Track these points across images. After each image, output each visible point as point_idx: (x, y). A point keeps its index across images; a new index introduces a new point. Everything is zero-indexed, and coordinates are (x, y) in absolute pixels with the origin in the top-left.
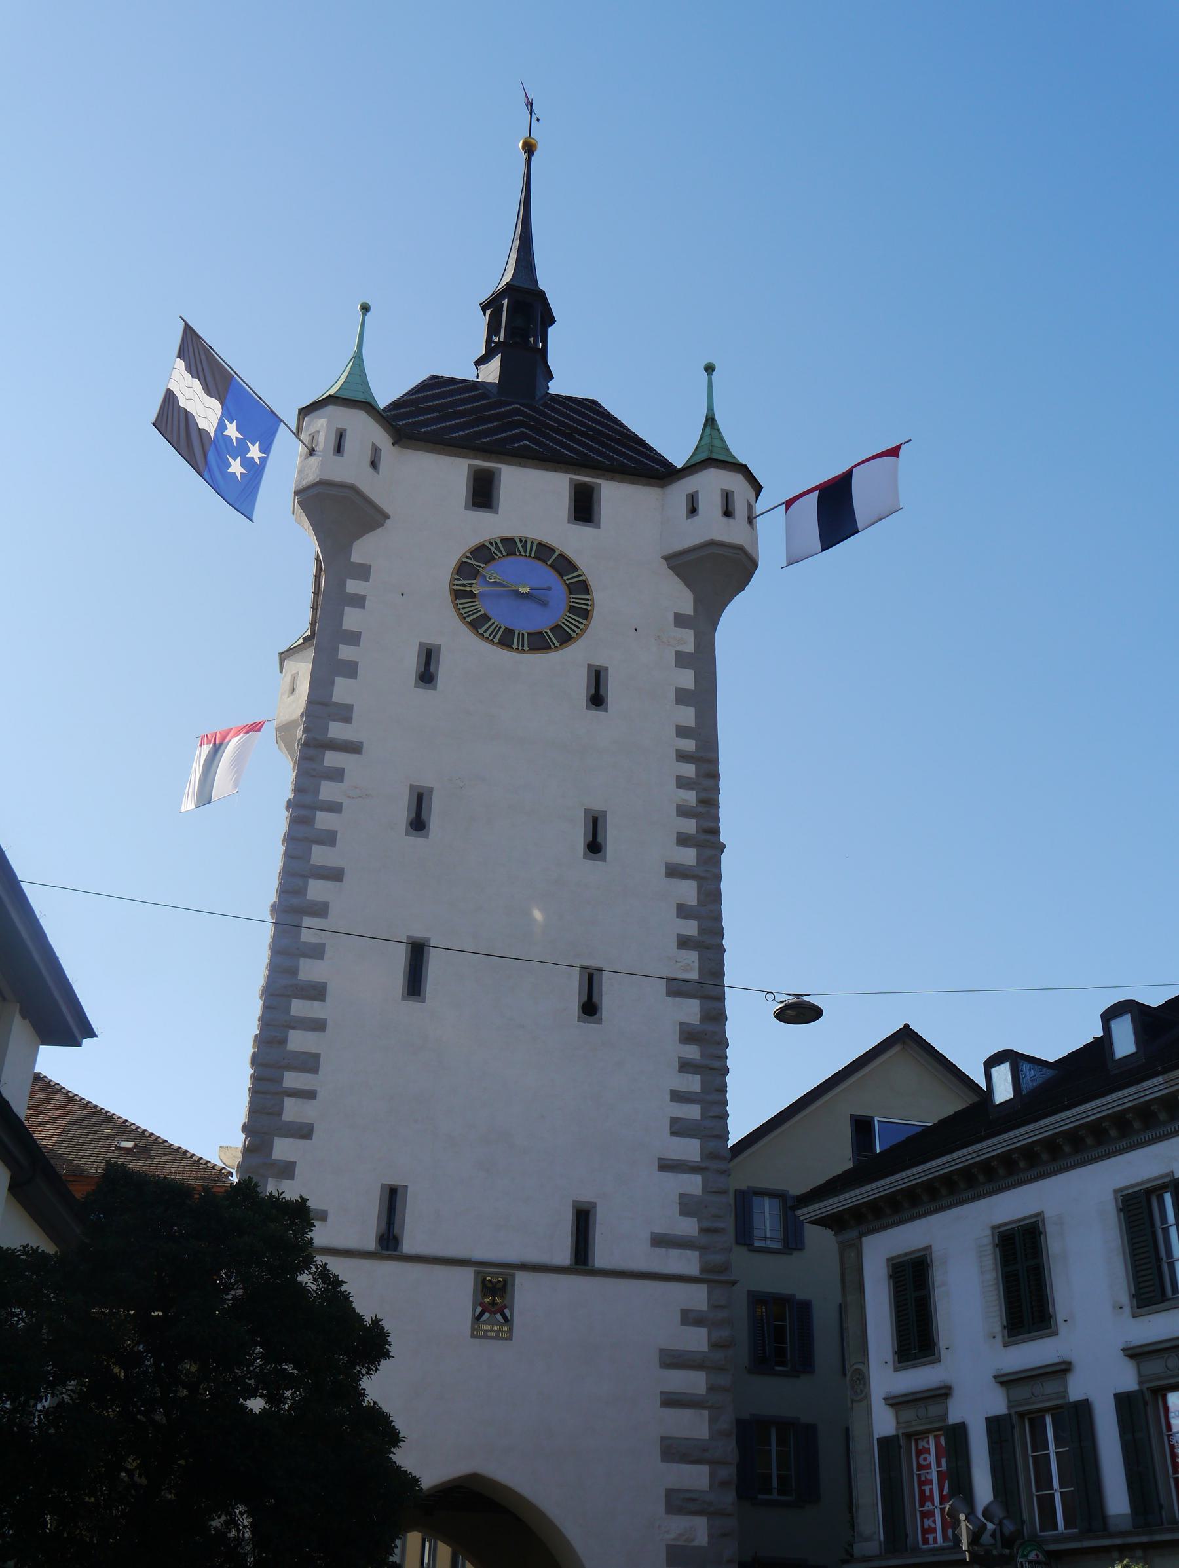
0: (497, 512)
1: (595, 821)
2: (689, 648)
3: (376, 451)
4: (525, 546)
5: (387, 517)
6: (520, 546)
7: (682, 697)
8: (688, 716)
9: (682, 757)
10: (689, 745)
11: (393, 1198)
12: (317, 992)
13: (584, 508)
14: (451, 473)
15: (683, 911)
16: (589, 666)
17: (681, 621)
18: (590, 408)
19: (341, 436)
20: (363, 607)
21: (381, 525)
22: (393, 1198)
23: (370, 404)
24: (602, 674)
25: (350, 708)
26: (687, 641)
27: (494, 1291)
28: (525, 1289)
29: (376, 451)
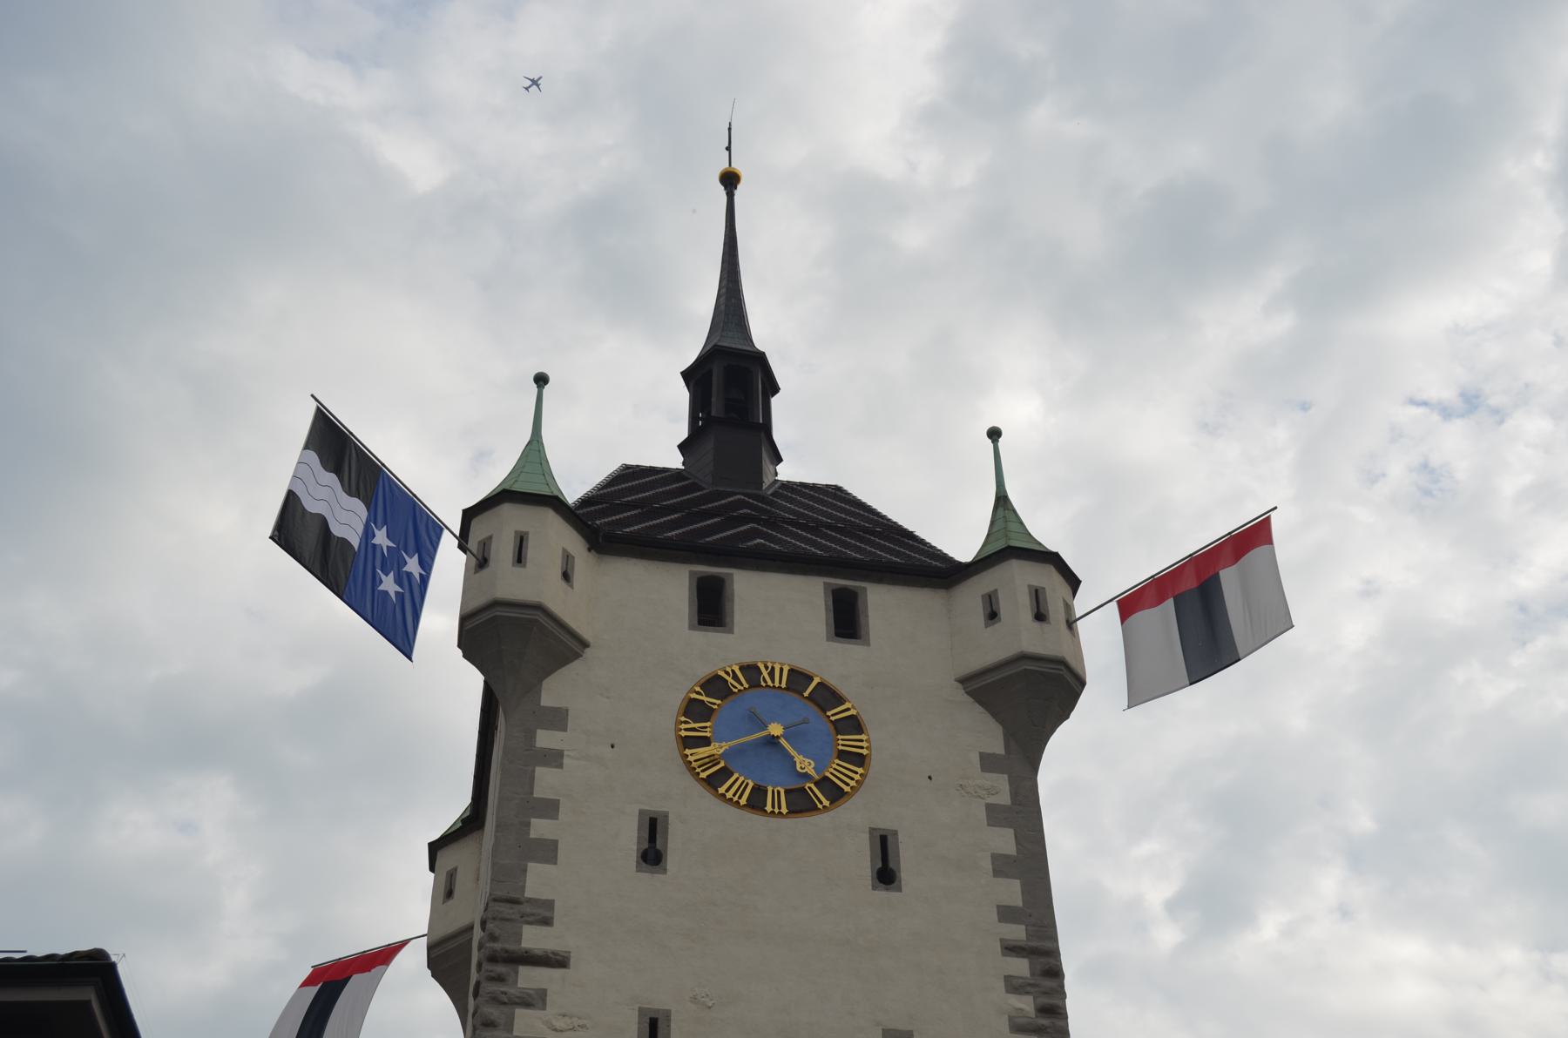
0: (731, 631)
2: (1004, 798)
3: (568, 558)
4: (772, 674)
5: (585, 645)
6: (765, 674)
7: (1002, 865)
8: (1011, 892)
9: (1011, 949)
10: (1017, 933)
13: (847, 621)
16: (872, 830)
17: (989, 763)
18: (835, 497)
19: (521, 541)
20: (560, 766)
21: (577, 656)
23: (556, 498)
24: (890, 839)
25: (549, 905)
26: (1000, 789)
29: (568, 558)
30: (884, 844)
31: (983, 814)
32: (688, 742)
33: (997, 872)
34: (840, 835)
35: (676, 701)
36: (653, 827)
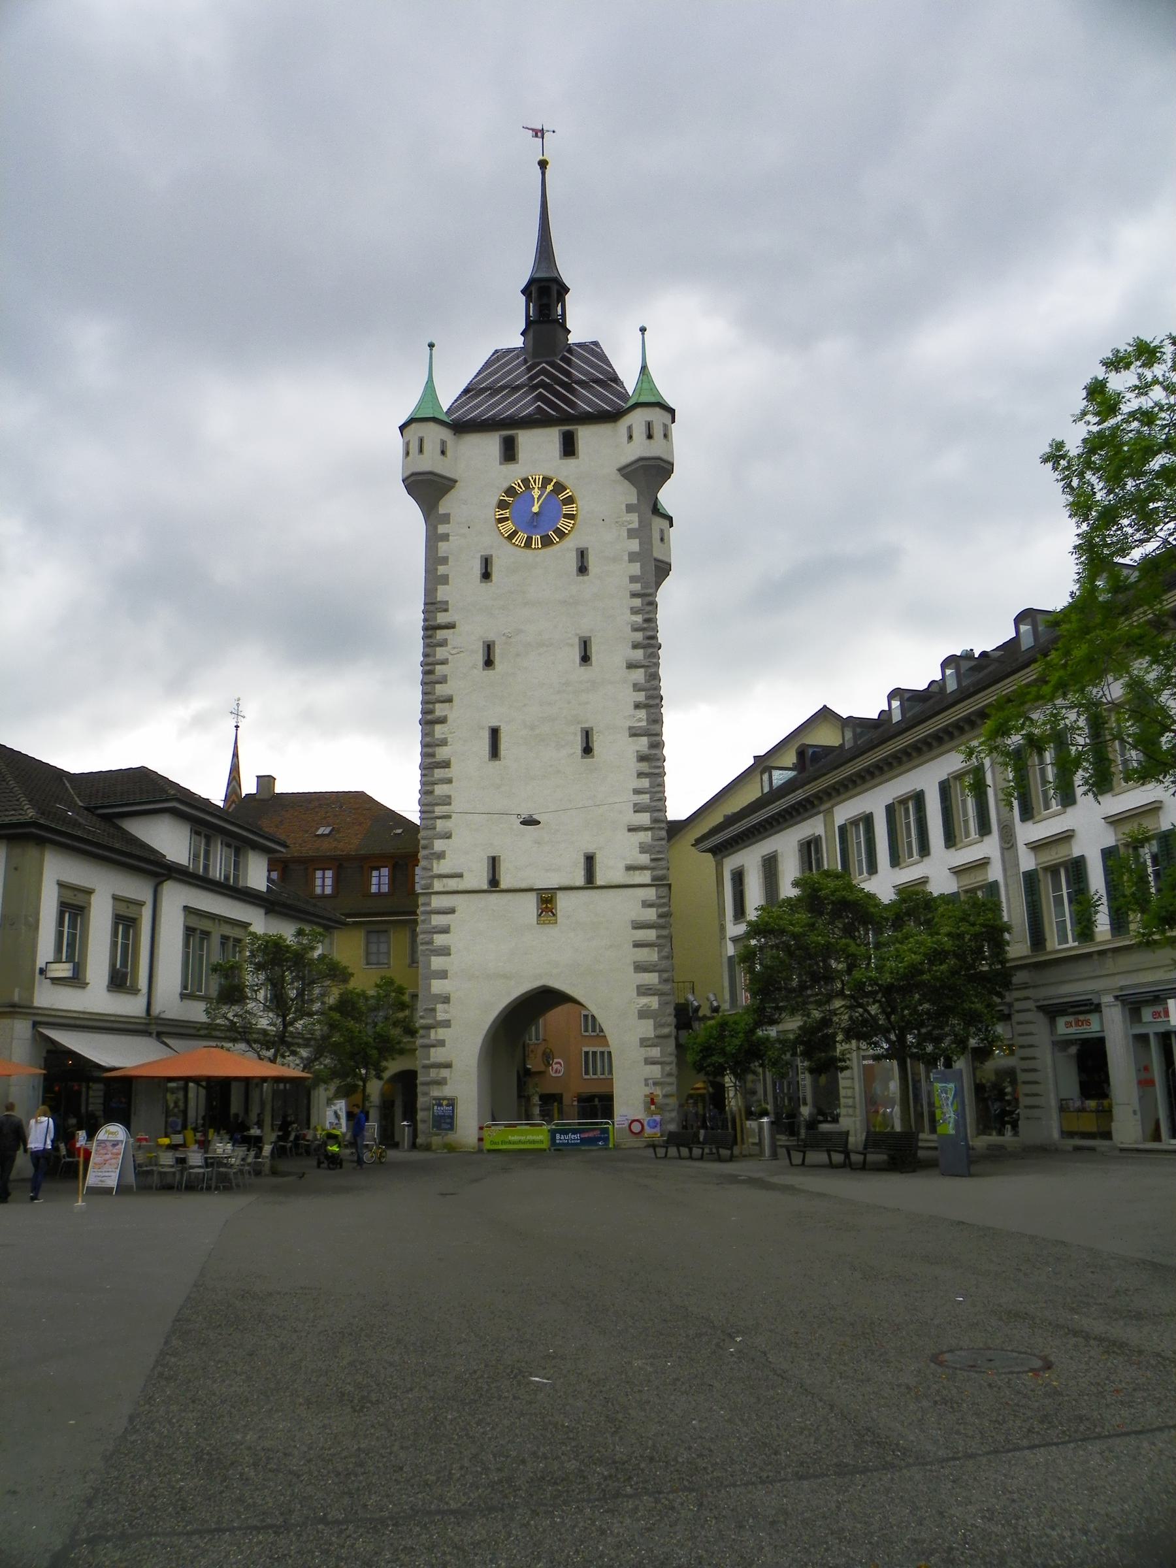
1: (585, 643)
2: (635, 525)
5: (456, 481)
9: (634, 595)
11: (494, 862)
12: (446, 764)
13: (569, 448)
14: (491, 444)
15: (637, 687)
22: (494, 862)
27: (547, 901)
28: (563, 902)
29: (443, 443)
30: (582, 554)
31: (625, 534)
32: (500, 521)
33: (630, 561)
34: (564, 553)
35: (494, 501)
36: (487, 562)
